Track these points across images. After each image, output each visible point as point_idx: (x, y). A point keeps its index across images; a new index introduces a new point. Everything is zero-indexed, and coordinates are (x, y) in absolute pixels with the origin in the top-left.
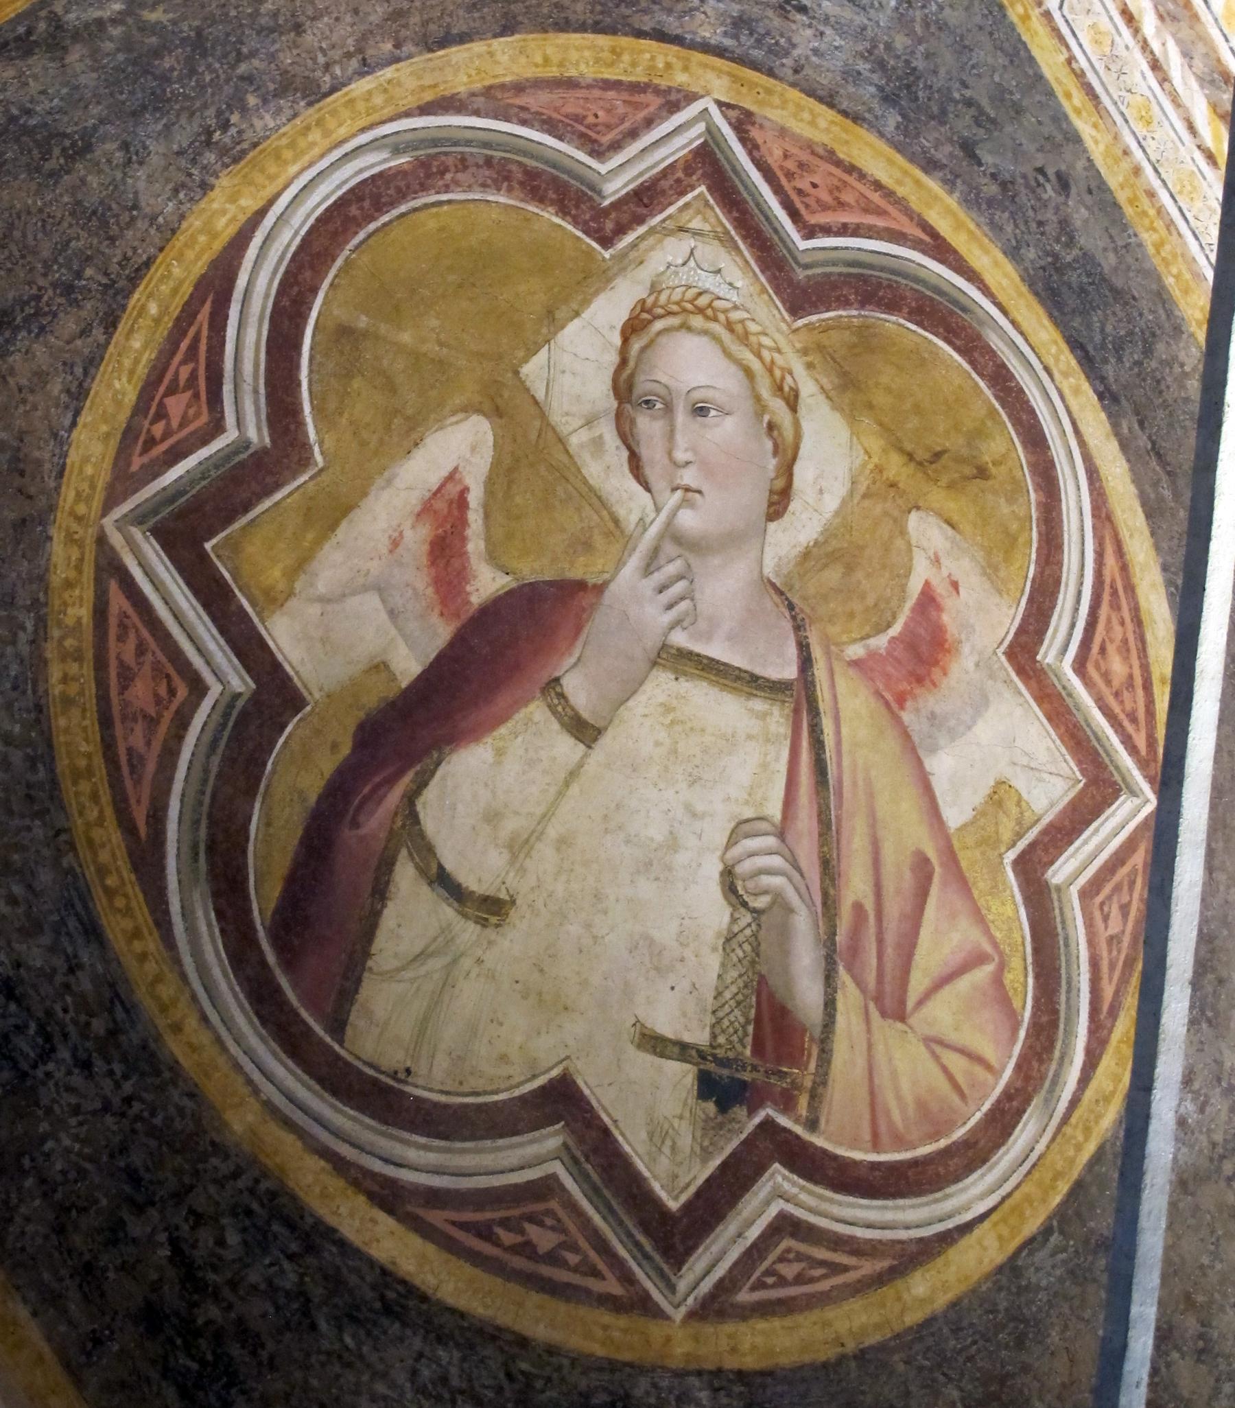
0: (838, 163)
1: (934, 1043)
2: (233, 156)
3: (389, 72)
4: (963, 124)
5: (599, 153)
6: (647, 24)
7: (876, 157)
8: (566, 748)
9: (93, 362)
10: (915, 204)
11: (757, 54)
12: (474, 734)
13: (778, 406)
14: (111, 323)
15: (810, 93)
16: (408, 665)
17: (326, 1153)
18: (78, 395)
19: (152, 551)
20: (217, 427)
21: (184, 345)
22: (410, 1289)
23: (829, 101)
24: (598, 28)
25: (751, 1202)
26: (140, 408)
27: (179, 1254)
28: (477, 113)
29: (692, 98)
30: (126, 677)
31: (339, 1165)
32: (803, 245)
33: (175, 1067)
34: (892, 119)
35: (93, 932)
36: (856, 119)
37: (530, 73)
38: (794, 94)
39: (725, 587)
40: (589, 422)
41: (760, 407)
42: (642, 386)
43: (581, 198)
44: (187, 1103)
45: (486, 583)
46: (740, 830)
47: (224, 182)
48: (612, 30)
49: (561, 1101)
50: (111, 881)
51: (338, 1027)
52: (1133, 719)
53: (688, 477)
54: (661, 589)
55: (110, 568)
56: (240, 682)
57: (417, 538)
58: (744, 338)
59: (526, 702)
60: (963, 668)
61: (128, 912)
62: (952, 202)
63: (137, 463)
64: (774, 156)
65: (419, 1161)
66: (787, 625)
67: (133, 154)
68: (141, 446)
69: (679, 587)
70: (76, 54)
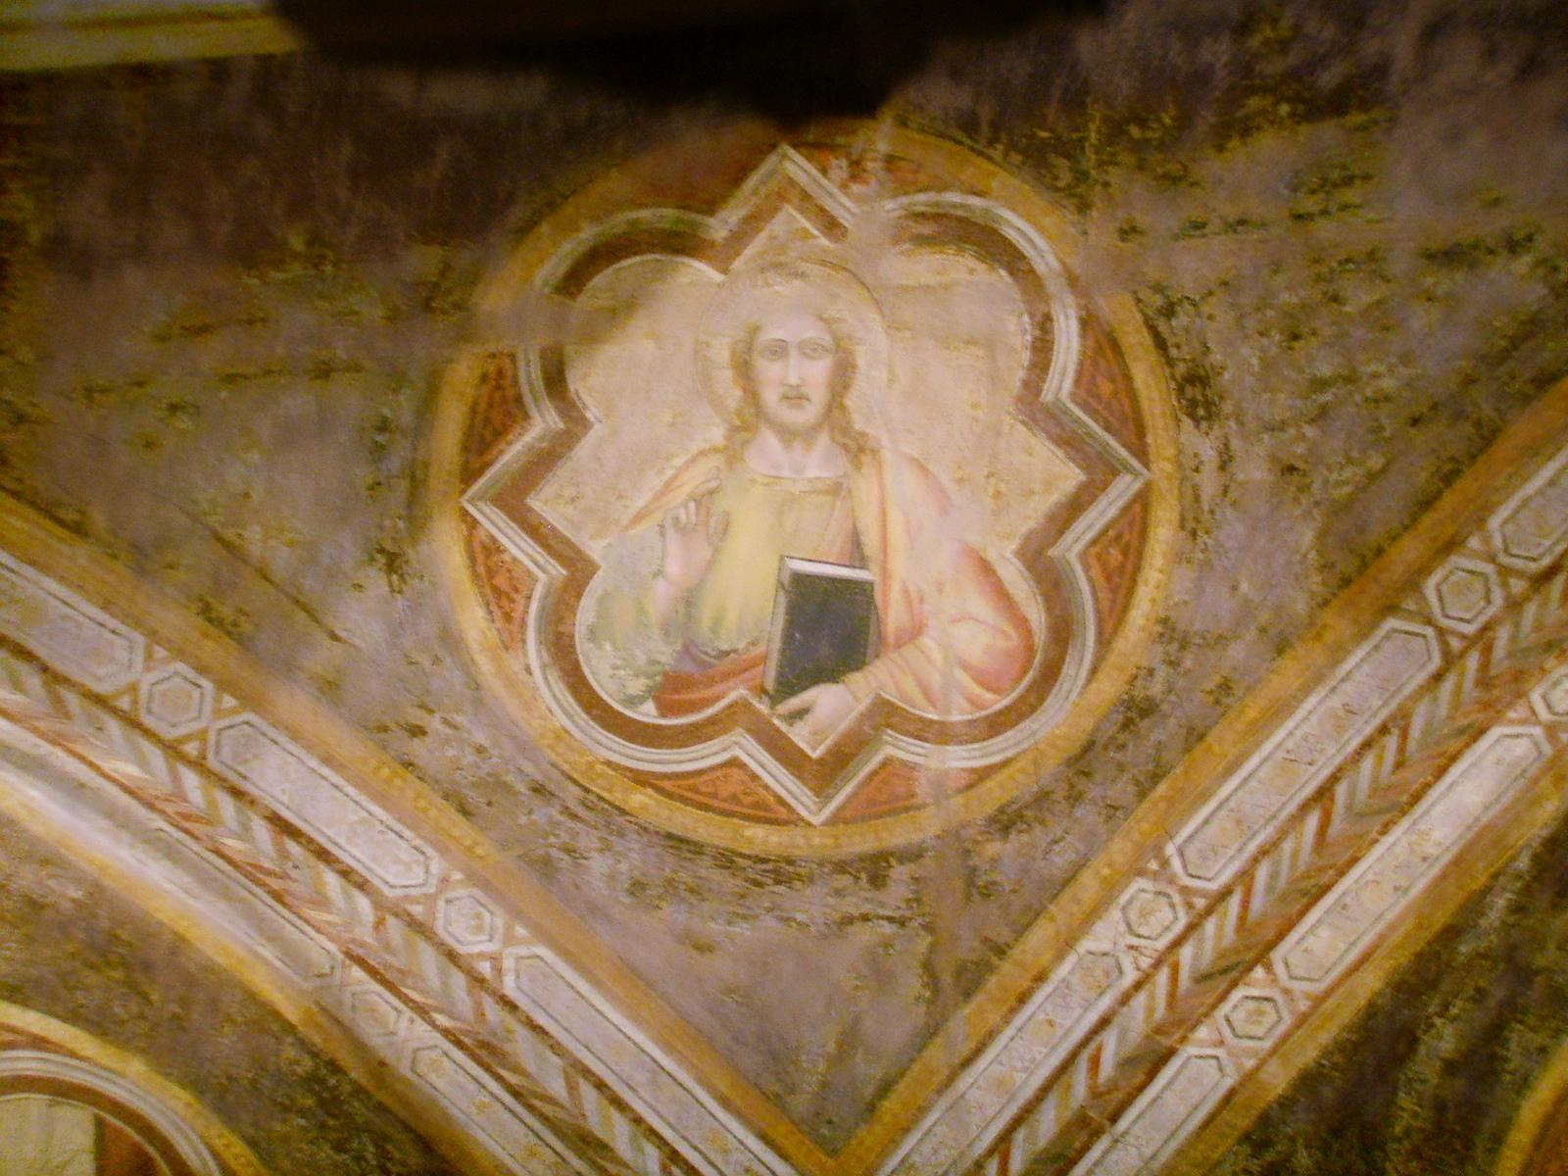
17: (82, 1059)
27: (146, 998)
31: (73, 1055)
33: (183, 1086)
35: (252, 1144)
44: (168, 1070)
51: (100, 1123)
61: (236, 1157)
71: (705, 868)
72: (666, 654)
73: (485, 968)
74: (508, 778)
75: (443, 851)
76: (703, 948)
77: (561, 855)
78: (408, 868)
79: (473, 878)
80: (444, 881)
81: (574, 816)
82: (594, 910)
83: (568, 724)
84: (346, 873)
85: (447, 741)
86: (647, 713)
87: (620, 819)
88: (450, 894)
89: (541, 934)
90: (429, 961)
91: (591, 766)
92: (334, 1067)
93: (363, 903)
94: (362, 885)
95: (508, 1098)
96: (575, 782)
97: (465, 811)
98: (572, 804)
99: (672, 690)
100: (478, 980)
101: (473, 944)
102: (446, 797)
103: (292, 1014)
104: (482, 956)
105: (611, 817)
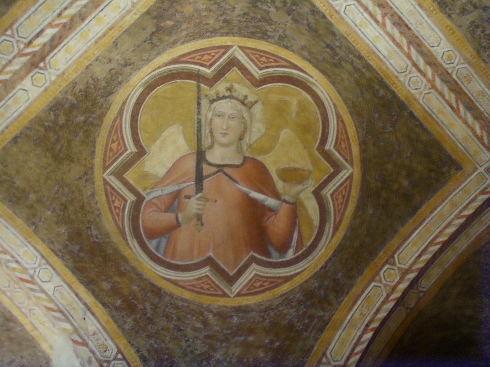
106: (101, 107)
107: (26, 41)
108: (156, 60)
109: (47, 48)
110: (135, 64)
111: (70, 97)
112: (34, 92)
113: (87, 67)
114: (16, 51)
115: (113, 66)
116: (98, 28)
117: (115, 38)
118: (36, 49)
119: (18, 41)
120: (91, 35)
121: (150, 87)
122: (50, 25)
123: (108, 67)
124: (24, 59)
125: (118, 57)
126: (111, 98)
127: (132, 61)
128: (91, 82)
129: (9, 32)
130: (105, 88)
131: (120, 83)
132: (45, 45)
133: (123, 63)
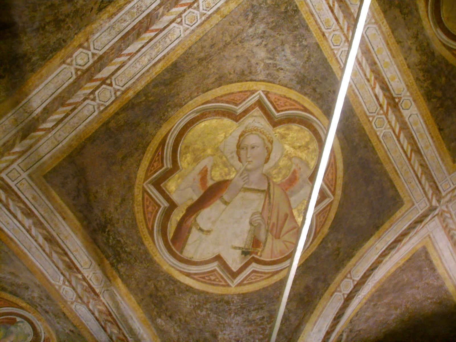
0: (286, 98)
1: (284, 242)
2: (166, 120)
3: (196, 99)
4: (314, 85)
5: (237, 105)
6: (249, 79)
7: (294, 95)
8: (223, 206)
9: (141, 160)
10: (301, 102)
11: (271, 80)
12: (207, 207)
13: (269, 145)
14: (144, 153)
15: (282, 85)
16: (196, 198)
17: (178, 270)
18: (138, 166)
19: (152, 187)
20: (163, 166)
21: (157, 154)
22: (191, 287)
23: (286, 86)
24: (238, 82)
25: (250, 267)
26: (149, 166)
27: (155, 286)
28: (213, 103)
29: (256, 91)
30: (148, 207)
32: (276, 114)
33: (155, 261)
34: (299, 87)
35: (143, 244)
36: (291, 88)
37: (224, 93)
38: (279, 86)
39: (255, 176)
40: (231, 153)
41: (265, 144)
42: (242, 146)
43: (232, 114)
44: (157, 266)
45: (210, 183)
46: (254, 214)
47: (164, 126)
48: (242, 81)
49: (218, 258)
50: (146, 236)
51: (181, 252)
52: (332, 185)
53: (250, 160)
54: (243, 179)
55: (145, 191)
56: (167, 205)
57: (198, 178)
58: (263, 133)
59: (216, 200)
60: (299, 182)
61: (148, 240)
62: (309, 101)
63: (149, 175)
64: (273, 99)
65: (193, 269)
66: (266, 181)
67: (147, 124)
68: (149, 171)
69: (246, 178)
70: (137, 109)
71: (10, 288)
72: (12, 328)
73: (67, 283)
74: (53, 316)
75: (71, 309)
76: (12, 274)
77: (44, 299)
78: (80, 309)
79: (66, 302)
80: (72, 303)
81: (40, 305)
82: (39, 286)
83: (38, 322)
84: (93, 314)
85: (66, 327)
86: (18, 319)
87: (28, 301)
88: (72, 300)
89: (53, 286)
90: (79, 290)
91: (34, 313)
92: (112, 265)
93: (91, 307)
94: (90, 310)
95: (69, 253)
96: (38, 311)
97: (64, 314)
98: (39, 307)
99: (13, 322)
100: (70, 282)
101: (68, 289)
102: (68, 318)
103: (119, 280)
104: (67, 286)
105: (31, 303)
106: (440, 63)
107: (379, 108)
108: (421, 13)
109: (387, 94)
110: (419, 30)
111: (426, 85)
112: (414, 109)
113: (409, 67)
114: (383, 116)
115: (414, 48)
116: (384, 53)
117: (395, 42)
118: (386, 102)
119: (378, 114)
120: (387, 60)
121: (439, 22)
122: (373, 89)
123: (414, 51)
124: (390, 112)
125: (409, 42)
126: (436, 54)
127: (416, 33)
128: (419, 67)
129: (371, 119)
130: (428, 57)
131: (428, 45)
132: (384, 95)
133: (415, 40)
